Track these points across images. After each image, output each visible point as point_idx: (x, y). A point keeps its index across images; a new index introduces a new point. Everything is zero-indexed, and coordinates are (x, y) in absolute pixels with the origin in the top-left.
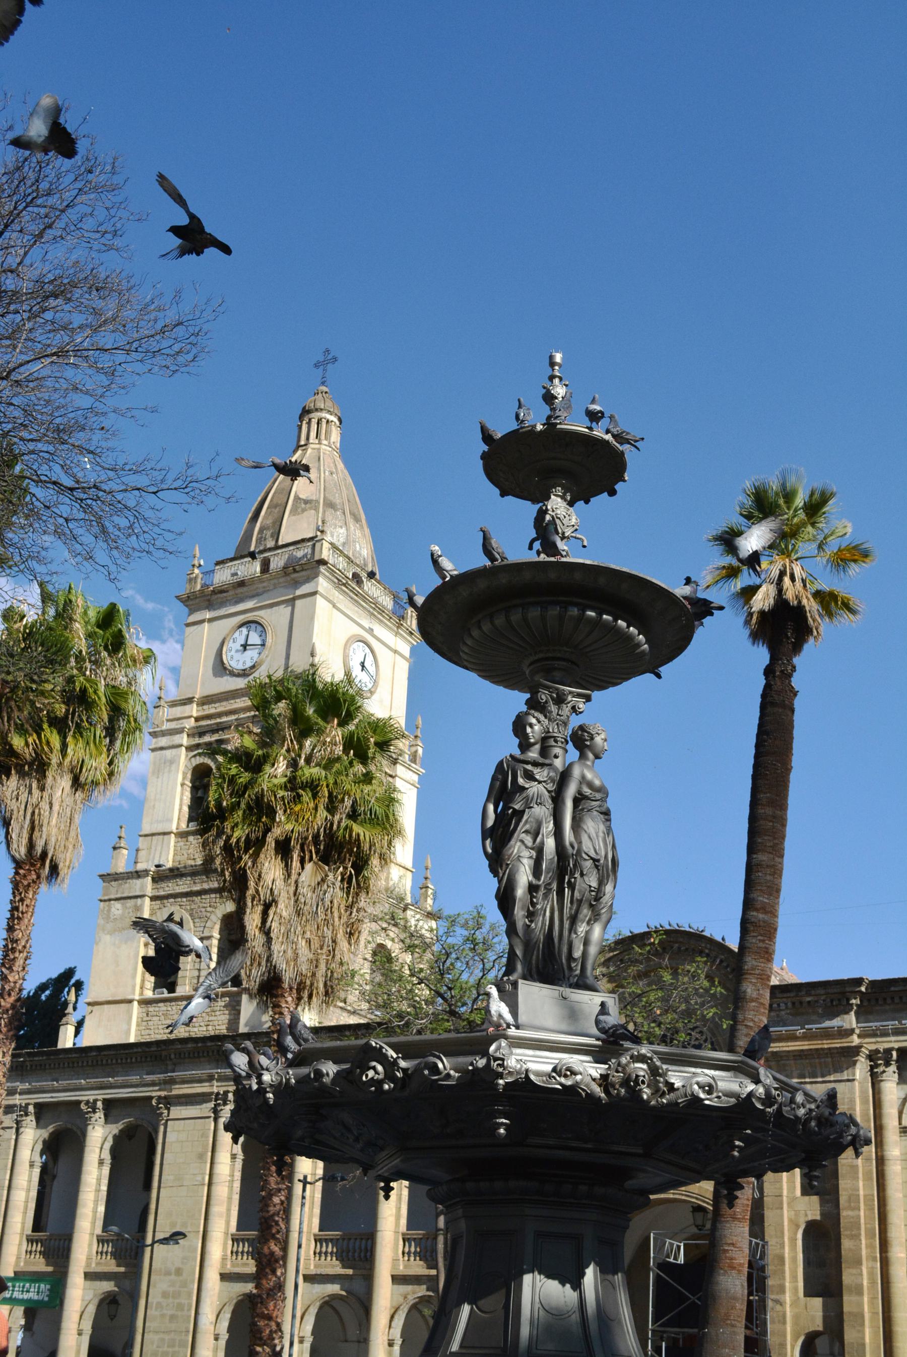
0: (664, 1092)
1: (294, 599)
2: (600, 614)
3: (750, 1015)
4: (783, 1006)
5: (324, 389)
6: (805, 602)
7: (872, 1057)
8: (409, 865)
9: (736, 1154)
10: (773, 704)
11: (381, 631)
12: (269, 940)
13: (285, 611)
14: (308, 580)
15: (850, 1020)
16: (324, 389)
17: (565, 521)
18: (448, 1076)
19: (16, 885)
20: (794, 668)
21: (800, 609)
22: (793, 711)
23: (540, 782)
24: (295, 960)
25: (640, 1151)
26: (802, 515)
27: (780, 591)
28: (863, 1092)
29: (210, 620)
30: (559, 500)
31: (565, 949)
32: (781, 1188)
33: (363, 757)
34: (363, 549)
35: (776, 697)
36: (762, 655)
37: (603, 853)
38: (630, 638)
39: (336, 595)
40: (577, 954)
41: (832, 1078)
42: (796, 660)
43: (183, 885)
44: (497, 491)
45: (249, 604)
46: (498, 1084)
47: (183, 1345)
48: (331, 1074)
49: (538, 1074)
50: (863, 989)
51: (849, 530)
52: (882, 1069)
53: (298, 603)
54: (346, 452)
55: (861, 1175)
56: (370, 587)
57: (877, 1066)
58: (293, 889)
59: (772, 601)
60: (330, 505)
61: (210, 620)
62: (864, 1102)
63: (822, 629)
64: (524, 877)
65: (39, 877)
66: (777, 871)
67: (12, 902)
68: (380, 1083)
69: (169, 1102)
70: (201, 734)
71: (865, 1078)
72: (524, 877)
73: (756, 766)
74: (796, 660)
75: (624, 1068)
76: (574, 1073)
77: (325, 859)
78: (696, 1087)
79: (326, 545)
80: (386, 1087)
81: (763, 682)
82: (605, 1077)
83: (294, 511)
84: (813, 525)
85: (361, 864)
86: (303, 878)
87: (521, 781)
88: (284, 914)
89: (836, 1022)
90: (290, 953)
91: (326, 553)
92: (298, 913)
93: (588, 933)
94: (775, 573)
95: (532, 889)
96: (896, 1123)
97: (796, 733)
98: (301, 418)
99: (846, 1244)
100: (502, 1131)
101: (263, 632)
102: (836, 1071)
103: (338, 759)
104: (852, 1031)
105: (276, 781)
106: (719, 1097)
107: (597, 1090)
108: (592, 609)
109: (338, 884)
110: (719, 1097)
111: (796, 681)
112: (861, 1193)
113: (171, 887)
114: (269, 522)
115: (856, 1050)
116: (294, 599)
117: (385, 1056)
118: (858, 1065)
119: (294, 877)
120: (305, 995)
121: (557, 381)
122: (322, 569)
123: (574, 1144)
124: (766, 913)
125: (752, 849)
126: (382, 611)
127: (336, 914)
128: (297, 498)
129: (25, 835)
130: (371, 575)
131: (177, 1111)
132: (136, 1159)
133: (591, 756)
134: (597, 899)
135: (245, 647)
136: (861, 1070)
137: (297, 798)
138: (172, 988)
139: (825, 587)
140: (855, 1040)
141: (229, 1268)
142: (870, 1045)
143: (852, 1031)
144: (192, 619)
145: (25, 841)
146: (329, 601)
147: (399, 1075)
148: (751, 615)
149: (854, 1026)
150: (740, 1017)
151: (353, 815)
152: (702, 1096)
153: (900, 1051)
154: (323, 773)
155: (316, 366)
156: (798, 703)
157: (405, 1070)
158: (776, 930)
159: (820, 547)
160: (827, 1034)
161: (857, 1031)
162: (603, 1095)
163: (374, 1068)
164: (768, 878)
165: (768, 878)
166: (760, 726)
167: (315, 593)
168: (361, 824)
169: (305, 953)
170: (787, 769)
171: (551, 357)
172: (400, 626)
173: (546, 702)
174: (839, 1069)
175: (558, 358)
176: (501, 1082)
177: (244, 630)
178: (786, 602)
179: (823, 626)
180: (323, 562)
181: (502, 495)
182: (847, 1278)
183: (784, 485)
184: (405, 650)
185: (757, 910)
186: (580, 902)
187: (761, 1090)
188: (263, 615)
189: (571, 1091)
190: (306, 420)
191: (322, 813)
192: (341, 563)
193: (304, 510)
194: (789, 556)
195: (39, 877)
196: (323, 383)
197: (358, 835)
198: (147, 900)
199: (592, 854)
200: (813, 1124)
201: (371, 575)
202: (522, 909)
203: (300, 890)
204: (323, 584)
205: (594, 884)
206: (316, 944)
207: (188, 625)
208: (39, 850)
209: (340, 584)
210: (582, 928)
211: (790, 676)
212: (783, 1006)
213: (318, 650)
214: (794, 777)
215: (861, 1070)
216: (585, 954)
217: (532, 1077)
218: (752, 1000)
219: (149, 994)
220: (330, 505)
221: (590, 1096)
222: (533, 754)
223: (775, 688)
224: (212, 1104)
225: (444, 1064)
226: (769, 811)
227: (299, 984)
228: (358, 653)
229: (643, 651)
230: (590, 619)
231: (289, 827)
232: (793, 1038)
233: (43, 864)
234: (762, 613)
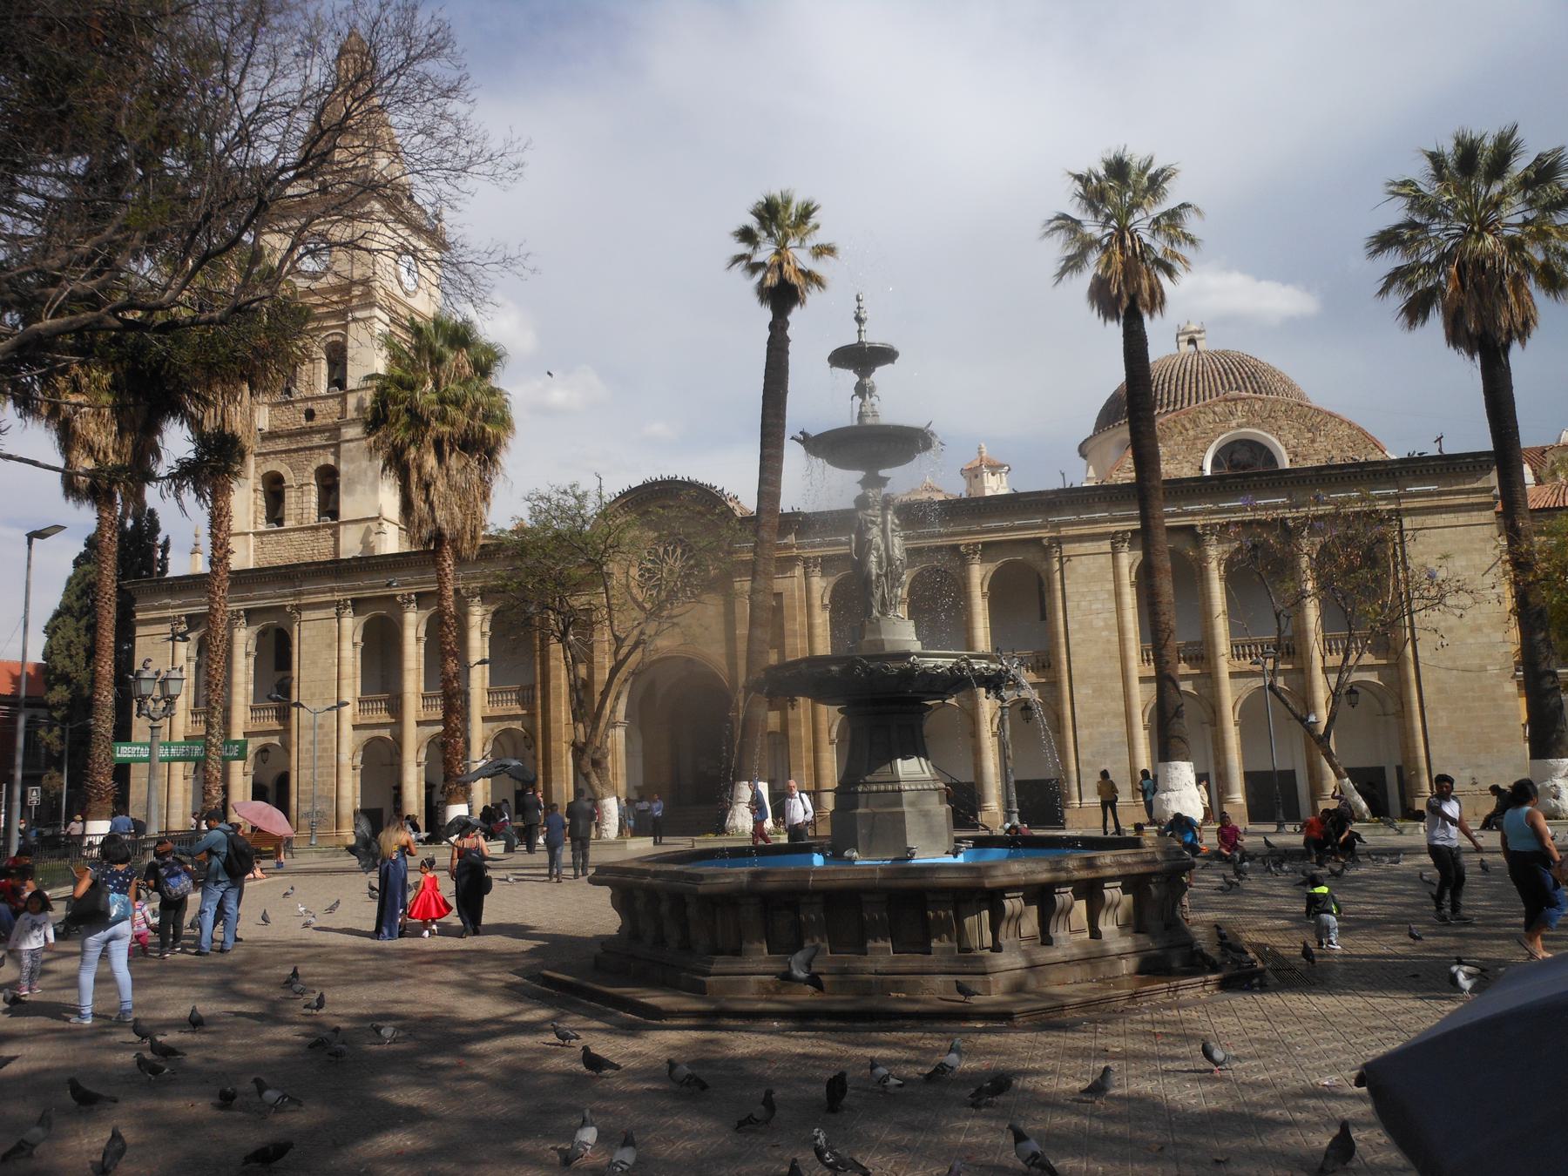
15: (791, 539)
36: (766, 314)
43: (281, 445)
47: (330, 775)
62: (800, 590)
69: (299, 608)
111: (790, 332)
113: (270, 446)
115: (797, 558)
131: (306, 615)
132: (277, 653)
136: (798, 571)
138: (280, 522)
141: (359, 721)
215: (798, 571)
219: (262, 528)
224: (334, 610)
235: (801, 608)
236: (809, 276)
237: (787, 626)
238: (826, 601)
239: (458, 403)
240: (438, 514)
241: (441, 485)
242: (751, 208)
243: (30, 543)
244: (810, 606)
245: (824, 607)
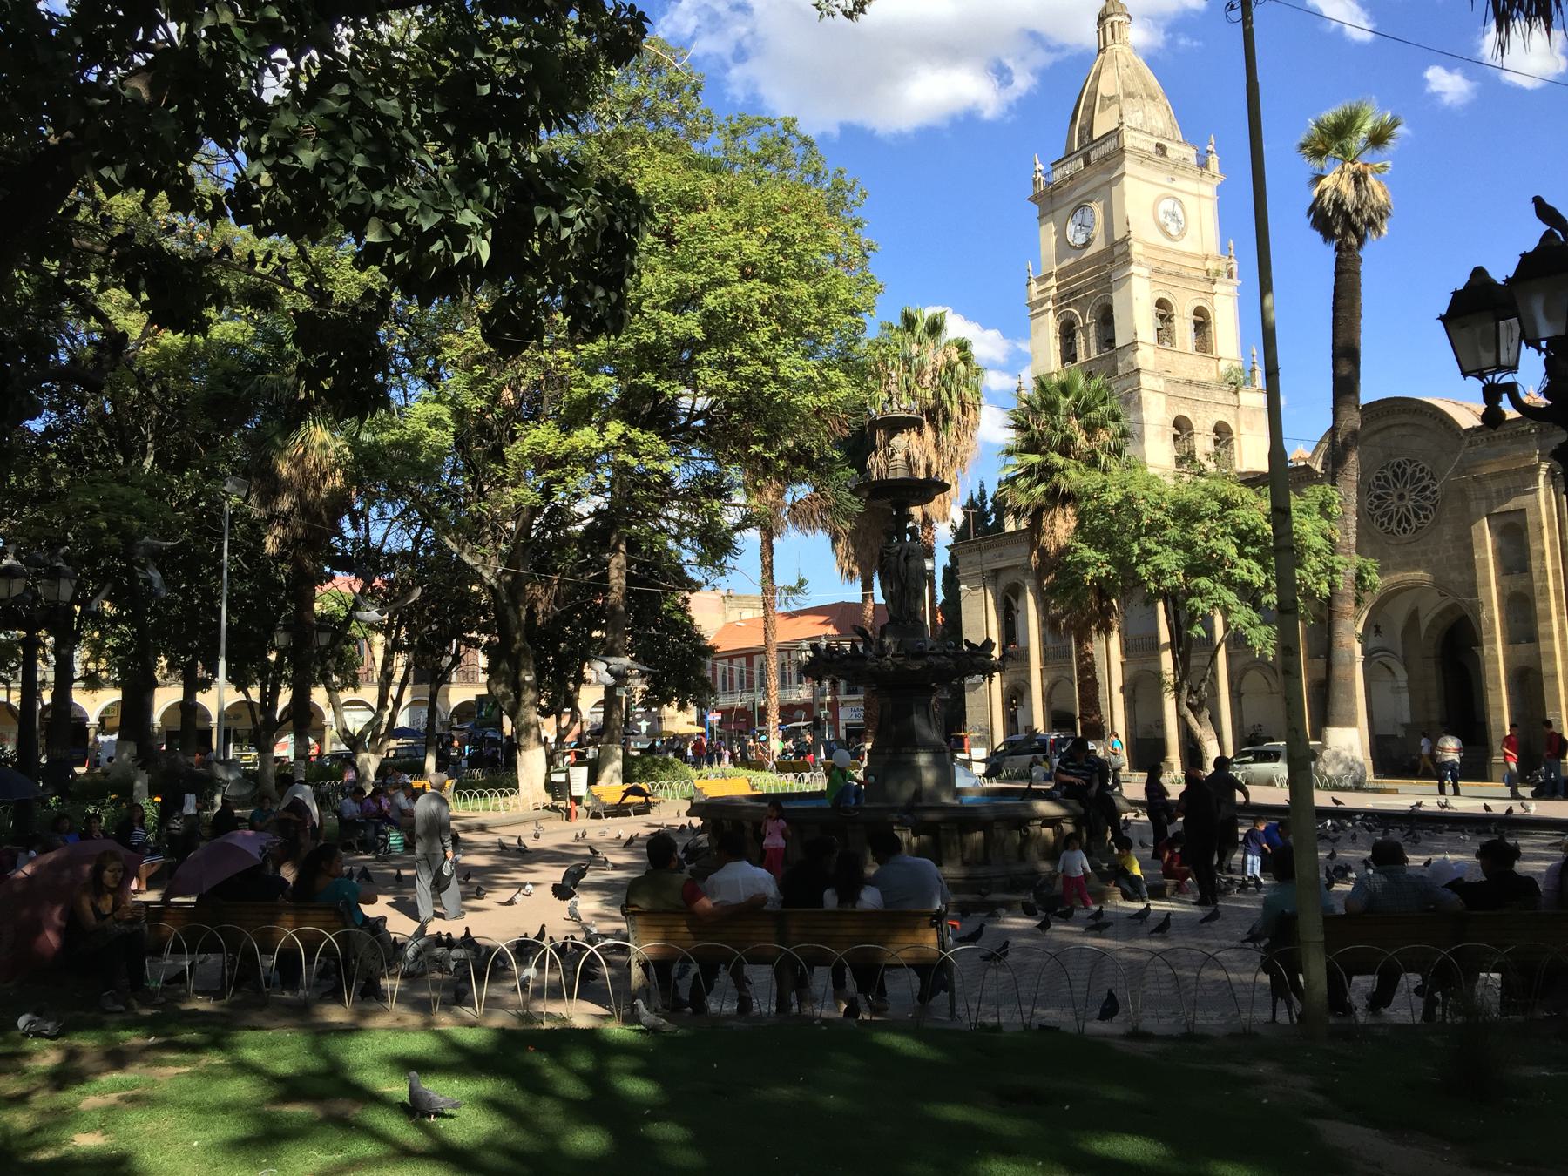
39: (1141, 171)
60: (1129, 95)
70: (1062, 299)
83: (1102, 109)
99: (1539, 605)
182: (1541, 628)
204: (1129, 165)
209: (1145, 158)
220: (1129, 95)
228: (1167, 205)
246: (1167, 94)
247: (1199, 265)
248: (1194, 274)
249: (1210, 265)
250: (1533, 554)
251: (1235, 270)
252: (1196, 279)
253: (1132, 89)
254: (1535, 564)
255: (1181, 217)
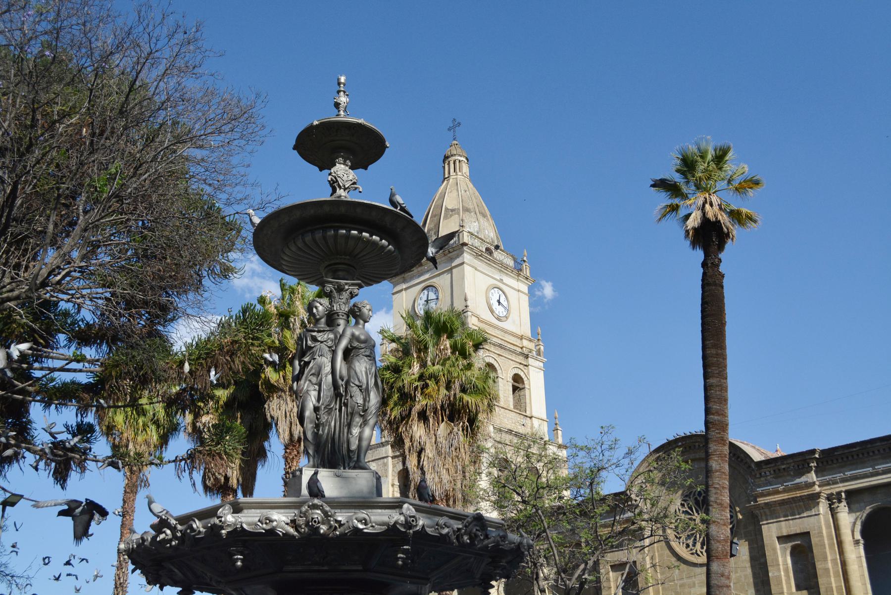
0: (336, 528)
1: (451, 269)
2: (360, 232)
3: (716, 481)
4: (768, 473)
5: (456, 142)
6: (720, 217)
7: (829, 498)
8: (544, 417)
9: (400, 563)
10: (709, 284)
11: (507, 280)
12: (423, 473)
13: (447, 277)
14: (458, 256)
15: (812, 477)
16: (456, 142)
17: (345, 178)
18: (200, 532)
19: (286, 458)
20: (720, 261)
21: (718, 222)
22: (722, 287)
23: (322, 342)
24: (441, 482)
25: (361, 568)
26: (713, 165)
27: (704, 214)
28: (827, 522)
29: (406, 289)
30: (342, 166)
31: (345, 445)
32: (782, 588)
33: (464, 354)
34: (490, 232)
35: (710, 280)
36: (699, 255)
37: (365, 382)
38: (375, 243)
39: (476, 263)
40: (354, 447)
41: (805, 515)
42: (720, 256)
44: (317, 169)
45: (427, 276)
46: (221, 534)
48: (149, 539)
49: (249, 524)
50: (817, 456)
51: (746, 169)
52: (836, 505)
53: (454, 271)
54: (474, 178)
55: (832, 574)
56: (497, 255)
57: (833, 503)
58: (434, 440)
59: (699, 221)
60: (466, 210)
61: (406, 289)
62: (828, 527)
63: (734, 233)
64: (311, 402)
65: (298, 453)
66: (724, 389)
67: (285, 469)
68: (170, 541)
71: (826, 512)
72: (311, 402)
73: (703, 324)
74: (720, 256)
75: (305, 514)
76: (271, 521)
77: (451, 419)
78: (355, 521)
79: (465, 234)
80: (173, 543)
81: (702, 270)
82: (293, 522)
83: (446, 218)
84: (720, 169)
85: (472, 421)
86: (439, 432)
87: (309, 342)
88: (430, 455)
89: (803, 479)
90: (437, 479)
91: (466, 238)
92: (439, 453)
93: (361, 433)
94: (700, 202)
95: (316, 409)
96: (851, 538)
97: (726, 301)
98: (444, 162)
100: (239, 563)
101: (437, 290)
102: (807, 510)
103: (449, 358)
104: (814, 483)
105: (413, 377)
106: (372, 526)
107: (291, 531)
108: (343, 228)
109: (460, 433)
110: (372, 526)
111: (722, 269)
112: (834, 585)
114: (432, 226)
115: (817, 496)
116: (451, 269)
117: (169, 523)
118: (821, 504)
119: (432, 432)
120: (451, 503)
121: (342, 93)
122: (465, 248)
123: (316, 568)
124: (719, 415)
125: (706, 376)
126: (506, 267)
127: (462, 450)
128: (447, 209)
129: (287, 430)
130: (497, 247)
133: (361, 322)
134: (365, 411)
135: (427, 301)
136: (823, 507)
137: (426, 386)
139: (734, 207)
140: (817, 489)
142: (827, 491)
143: (814, 483)
144: (396, 290)
145: (287, 433)
146: (473, 267)
147: (179, 534)
148: (687, 232)
149: (815, 479)
150: (710, 483)
151: (463, 390)
152: (361, 526)
153: (846, 492)
154: (441, 368)
155: (449, 130)
156: (726, 282)
157: (181, 531)
158: (727, 425)
159: (729, 182)
160: (798, 487)
161: (817, 483)
162: (296, 533)
163: (164, 532)
164: (718, 393)
165: (718, 393)
166: (703, 299)
167: (463, 263)
168: (470, 394)
169: (446, 478)
170: (723, 324)
171: (338, 79)
172: (519, 275)
173: (331, 291)
174: (809, 508)
175: (343, 79)
176: (223, 532)
177: (426, 292)
178: (708, 220)
179: (736, 231)
180: (465, 244)
181: (321, 170)
183: (699, 149)
184: (525, 289)
185: (713, 414)
186: (352, 414)
187: (402, 518)
188: (436, 281)
189: (272, 532)
190: (447, 162)
191: (443, 391)
192: (477, 243)
193: (451, 216)
194: (708, 191)
195: (298, 453)
196: (454, 139)
197: (468, 402)
198: (390, 459)
199: (357, 383)
200: (466, 538)
201: (497, 247)
202: (311, 423)
203: (438, 440)
204: (467, 257)
205: (360, 401)
206: (452, 471)
207: (393, 294)
208: (296, 437)
209: (478, 255)
210: (355, 431)
211: (718, 266)
212: (768, 473)
213: (469, 297)
214: (727, 328)
215: (823, 507)
216: (359, 446)
217: (245, 526)
218: (717, 471)
220: (466, 210)
221: (286, 535)
222: (322, 324)
223: (709, 274)
225: (197, 525)
226: (713, 351)
227: (447, 496)
228: (495, 295)
229: (390, 251)
230: (343, 235)
231: (424, 403)
232: (777, 492)
233: (300, 445)
234: (694, 229)
235: (831, 546)
236: (736, 216)
237: (819, 566)
238: (858, 536)
239: (435, 377)
240: (428, 477)
241: (430, 452)
242: (675, 168)
243: (4, 510)
244: (840, 544)
245: (857, 542)
246: (491, 215)
247: (517, 342)
248: (515, 348)
249: (525, 343)
250: (819, 572)
251: (542, 348)
252: (513, 352)
253: (471, 207)
254: (821, 581)
255: (505, 303)
